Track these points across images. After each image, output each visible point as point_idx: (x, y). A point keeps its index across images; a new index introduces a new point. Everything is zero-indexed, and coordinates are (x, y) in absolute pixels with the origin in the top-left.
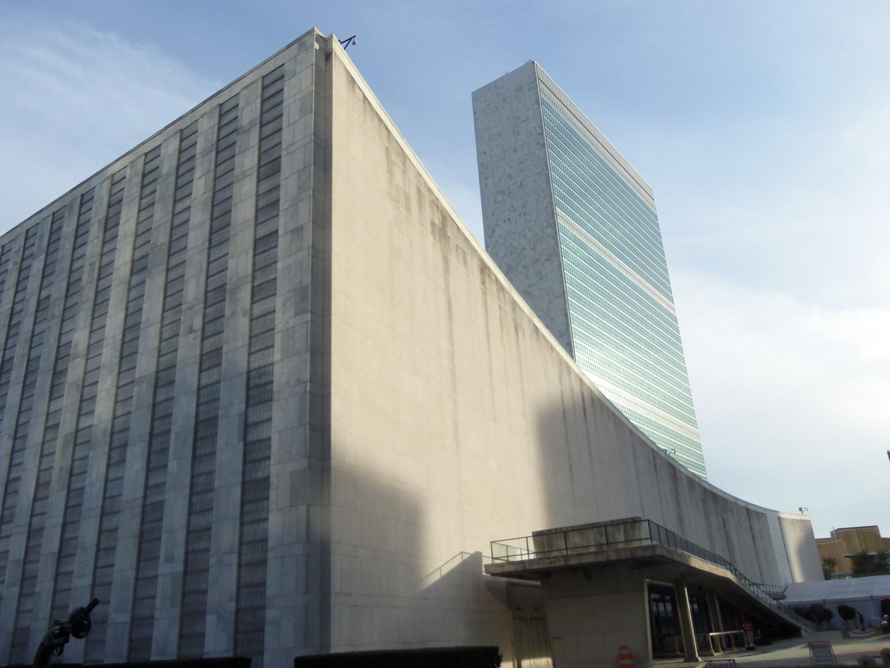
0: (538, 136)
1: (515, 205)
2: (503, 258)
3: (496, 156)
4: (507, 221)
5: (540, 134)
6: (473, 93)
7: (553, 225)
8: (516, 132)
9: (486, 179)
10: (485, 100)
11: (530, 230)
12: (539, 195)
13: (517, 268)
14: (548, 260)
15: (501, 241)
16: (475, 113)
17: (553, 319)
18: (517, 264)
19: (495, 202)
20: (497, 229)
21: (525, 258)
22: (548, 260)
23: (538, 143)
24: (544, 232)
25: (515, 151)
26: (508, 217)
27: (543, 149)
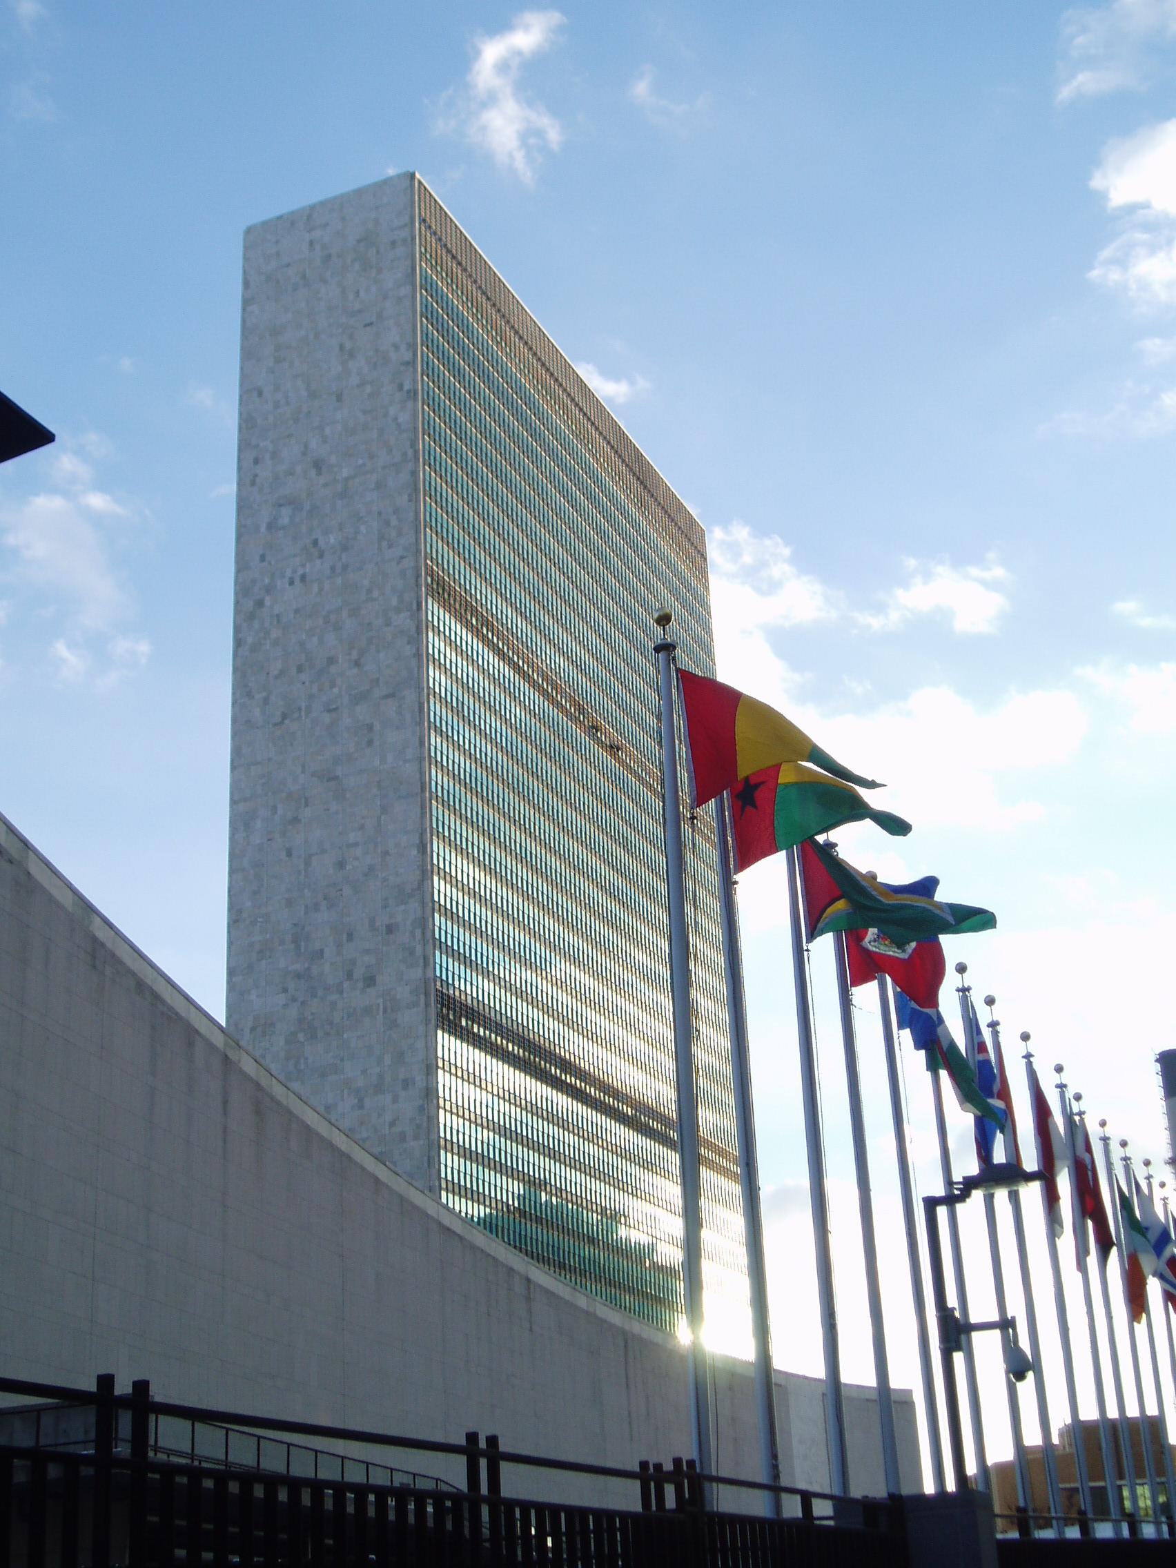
0: (402, 368)
1: (321, 543)
2: (276, 677)
3: (288, 404)
4: (297, 581)
5: (408, 363)
6: (249, 231)
8: (348, 345)
10: (278, 254)
12: (387, 523)
13: (309, 709)
15: (275, 633)
16: (246, 284)
17: (386, 853)
20: (268, 601)
21: (333, 685)
25: (339, 398)
26: (300, 571)
27: (410, 404)
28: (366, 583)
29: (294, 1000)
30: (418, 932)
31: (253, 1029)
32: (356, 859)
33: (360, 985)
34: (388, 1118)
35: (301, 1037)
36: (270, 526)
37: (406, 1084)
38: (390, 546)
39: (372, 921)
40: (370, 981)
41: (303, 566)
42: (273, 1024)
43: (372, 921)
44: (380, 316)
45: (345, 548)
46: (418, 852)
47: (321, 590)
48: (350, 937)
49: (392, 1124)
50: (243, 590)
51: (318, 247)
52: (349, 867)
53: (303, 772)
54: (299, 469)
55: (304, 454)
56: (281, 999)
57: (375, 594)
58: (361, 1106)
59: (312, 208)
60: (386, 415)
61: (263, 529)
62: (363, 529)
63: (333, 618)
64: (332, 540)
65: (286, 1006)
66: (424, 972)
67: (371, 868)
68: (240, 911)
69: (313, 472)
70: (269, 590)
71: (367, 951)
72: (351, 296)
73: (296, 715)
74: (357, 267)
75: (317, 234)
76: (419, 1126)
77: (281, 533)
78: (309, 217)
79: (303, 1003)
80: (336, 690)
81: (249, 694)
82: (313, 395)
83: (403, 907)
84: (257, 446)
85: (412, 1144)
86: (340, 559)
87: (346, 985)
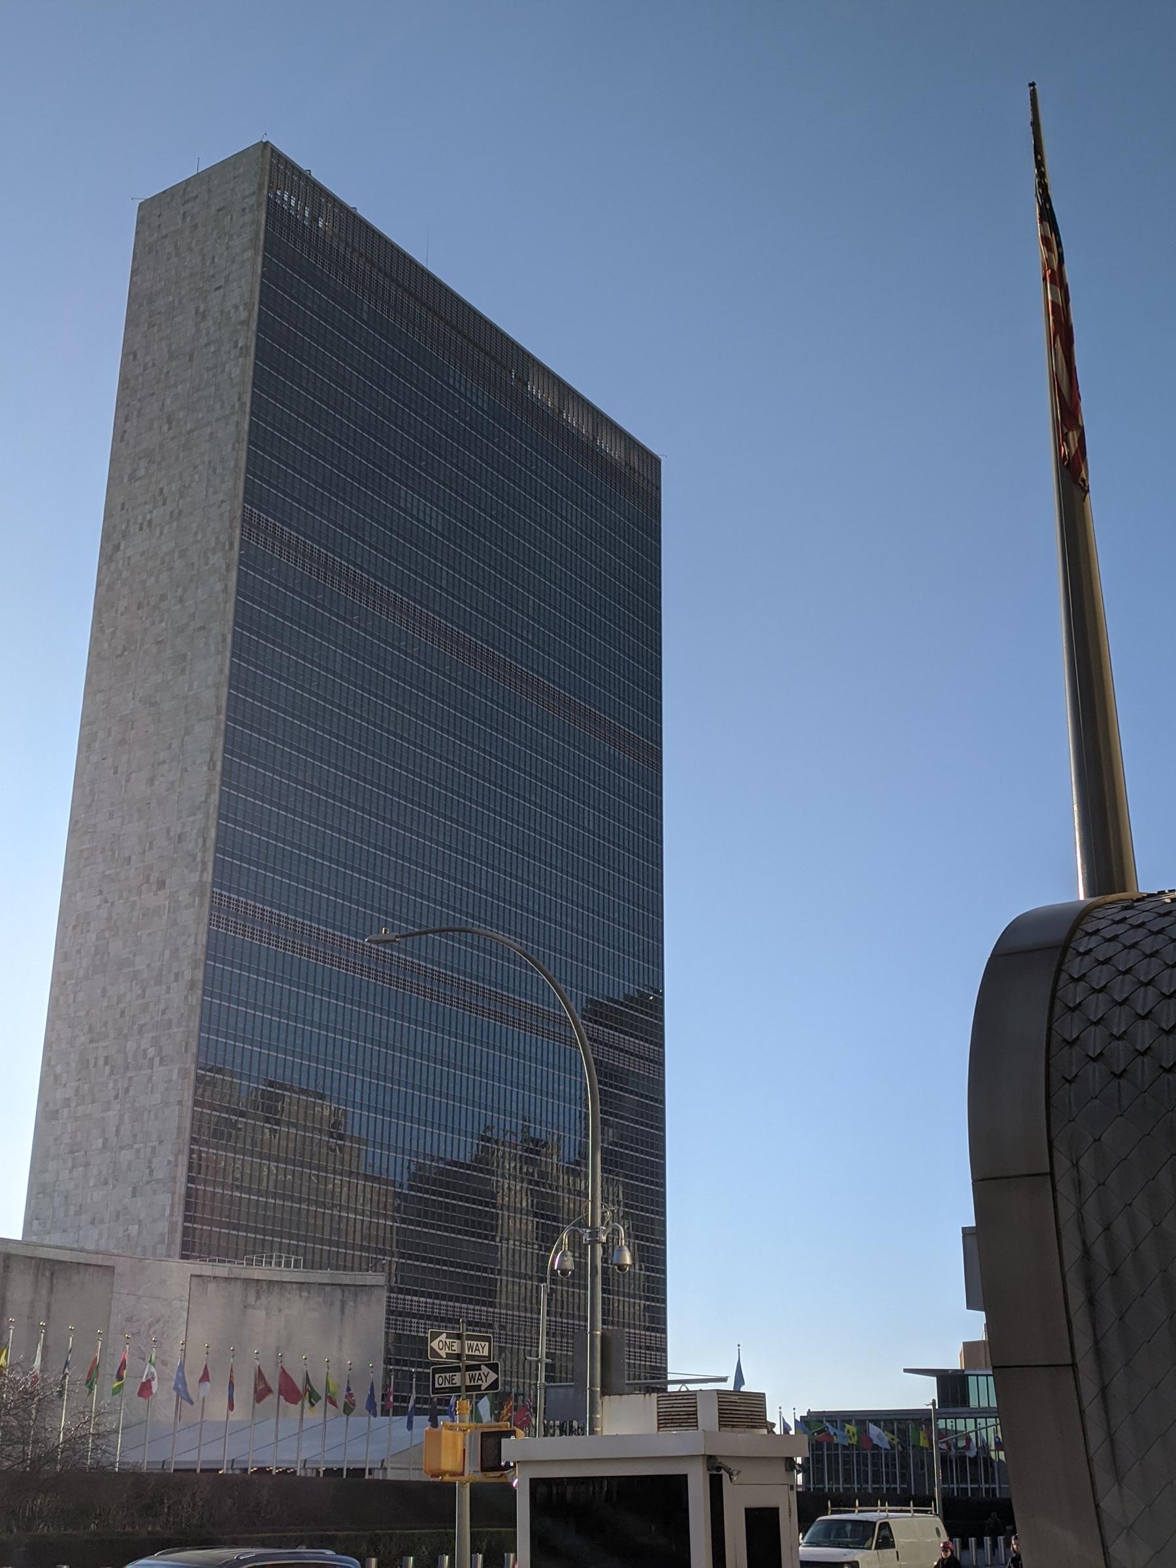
1: (165, 491)
5: (242, 323)
7: (227, 547)
8: (201, 310)
9: (126, 420)
10: (160, 225)
11: (183, 554)
12: (215, 473)
18: (146, 630)
19: (133, 477)
20: (122, 547)
21: (161, 621)
22: (202, 628)
23: (236, 346)
24: (207, 564)
25: (191, 360)
26: (148, 517)
28: (194, 526)
29: (106, 901)
30: (201, 840)
31: (75, 927)
33: (154, 887)
34: (162, 1007)
36: (130, 480)
38: (215, 493)
39: (168, 831)
40: (161, 884)
41: (151, 512)
42: (89, 923)
43: (168, 831)
44: (227, 278)
45: (182, 496)
46: (209, 769)
47: (161, 534)
49: (163, 1013)
50: (106, 537)
51: (188, 219)
52: (157, 783)
54: (156, 425)
55: (161, 410)
56: (98, 900)
57: (199, 537)
58: (143, 997)
60: (223, 371)
63: (167, 559)
64: (173, 489)
65: (99, 907)
66: (201, 876)
67: (172, 783)
68: (77, 822)
69: (166, 427)
72: (208, 263)
73: (133, 647)
74: (215, 232)
75: (190, 205)
77: (137, 483)
80: (163, 624)
81: (102, 630)
82: (172, 356)
83: (191, 819)
84: (128, 405)
85: (176, 1030)
86: (178, 505)
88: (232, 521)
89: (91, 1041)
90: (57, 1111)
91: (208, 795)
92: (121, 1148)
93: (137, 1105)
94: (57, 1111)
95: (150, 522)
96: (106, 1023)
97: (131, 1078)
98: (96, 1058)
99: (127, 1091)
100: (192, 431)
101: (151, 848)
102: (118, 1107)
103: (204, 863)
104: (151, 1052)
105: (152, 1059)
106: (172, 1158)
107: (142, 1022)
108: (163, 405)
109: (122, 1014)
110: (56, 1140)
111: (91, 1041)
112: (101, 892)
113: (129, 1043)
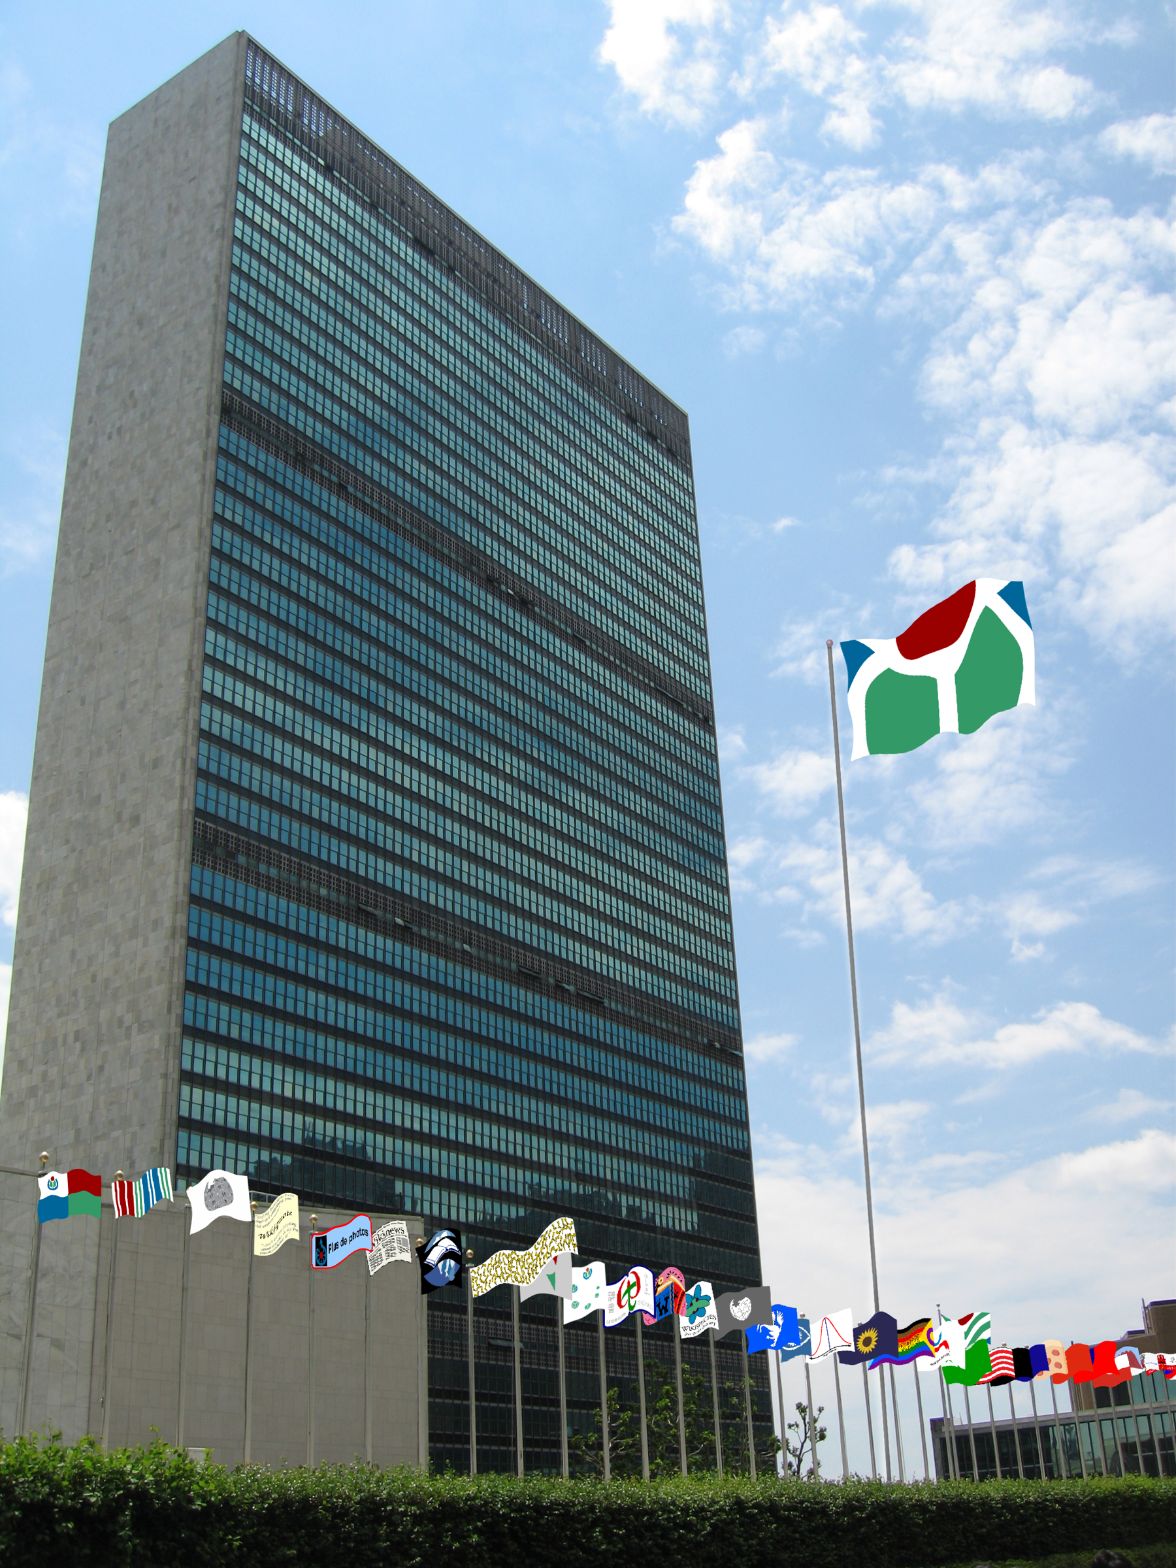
2: (90, 531)
4: (115, 437)
5: (218, 206)
7: (204, 435)
9: (95, 331)
10: (130, 139)
14: (178, 526)
17: (160, 686)
20: (90, 462)
22: (178, 526)
25: (164, 254)
26: (118, 425)
29: (73, 850)
30: (179, 762)
31: (39, 885)
32: (135, 696)
33: (127, 826)
35: (75, 888)
37: (156, 923)
38: (189, 382)
41: (120, 418)
48: (123, 776)
49: (141, 969)
52: (128, 706)
53: (102, 619)
57: (174, 431)
58: (116, 954)
59: (160, 89)
61: (93, 393)
62: (170, 371)
70: (93, 449)
71: (135, 790)
76: (163, 969)
78: (157, 98)
79: (81, 852)
80: (134, 532)
83: (168, 739)
87: (116, 827)
88: (209, 407)
89: (60, 1015)
90: (22, 1103)
91: (187, 709)
92: (97, 1138)
93: (113, 1085)
94: (22, 1103)
95: (119, 430)
96: (75, 993)
97: (106, 1053)
98: (65, 1036)
99: (101, 1069)
100: (165, 325)
101: (123, 780)
102: (91, 1090)
103: (183, 788)
104: (129, 1019)
105: (129, 1028)
106: (157, 1144)
107: (118, 985)
108: (134, 307)
109: (94, 978)
110: (21, 1138)
111: (60, 1015)
112: (67, 841)
113: (102, 1012)
